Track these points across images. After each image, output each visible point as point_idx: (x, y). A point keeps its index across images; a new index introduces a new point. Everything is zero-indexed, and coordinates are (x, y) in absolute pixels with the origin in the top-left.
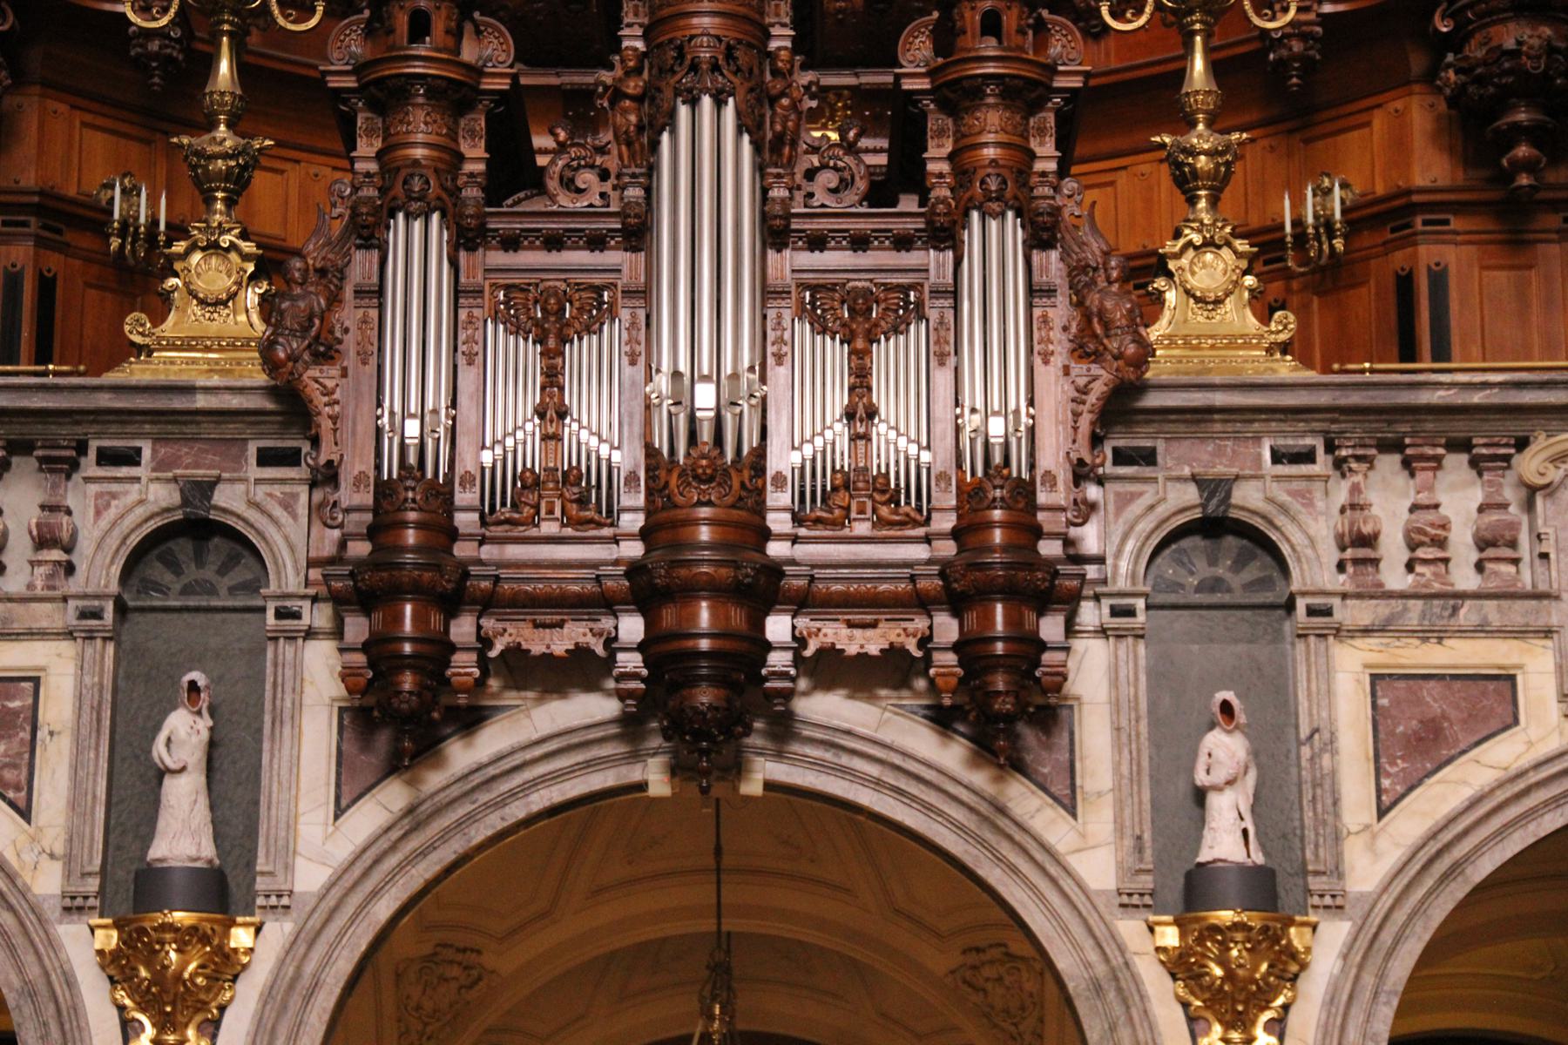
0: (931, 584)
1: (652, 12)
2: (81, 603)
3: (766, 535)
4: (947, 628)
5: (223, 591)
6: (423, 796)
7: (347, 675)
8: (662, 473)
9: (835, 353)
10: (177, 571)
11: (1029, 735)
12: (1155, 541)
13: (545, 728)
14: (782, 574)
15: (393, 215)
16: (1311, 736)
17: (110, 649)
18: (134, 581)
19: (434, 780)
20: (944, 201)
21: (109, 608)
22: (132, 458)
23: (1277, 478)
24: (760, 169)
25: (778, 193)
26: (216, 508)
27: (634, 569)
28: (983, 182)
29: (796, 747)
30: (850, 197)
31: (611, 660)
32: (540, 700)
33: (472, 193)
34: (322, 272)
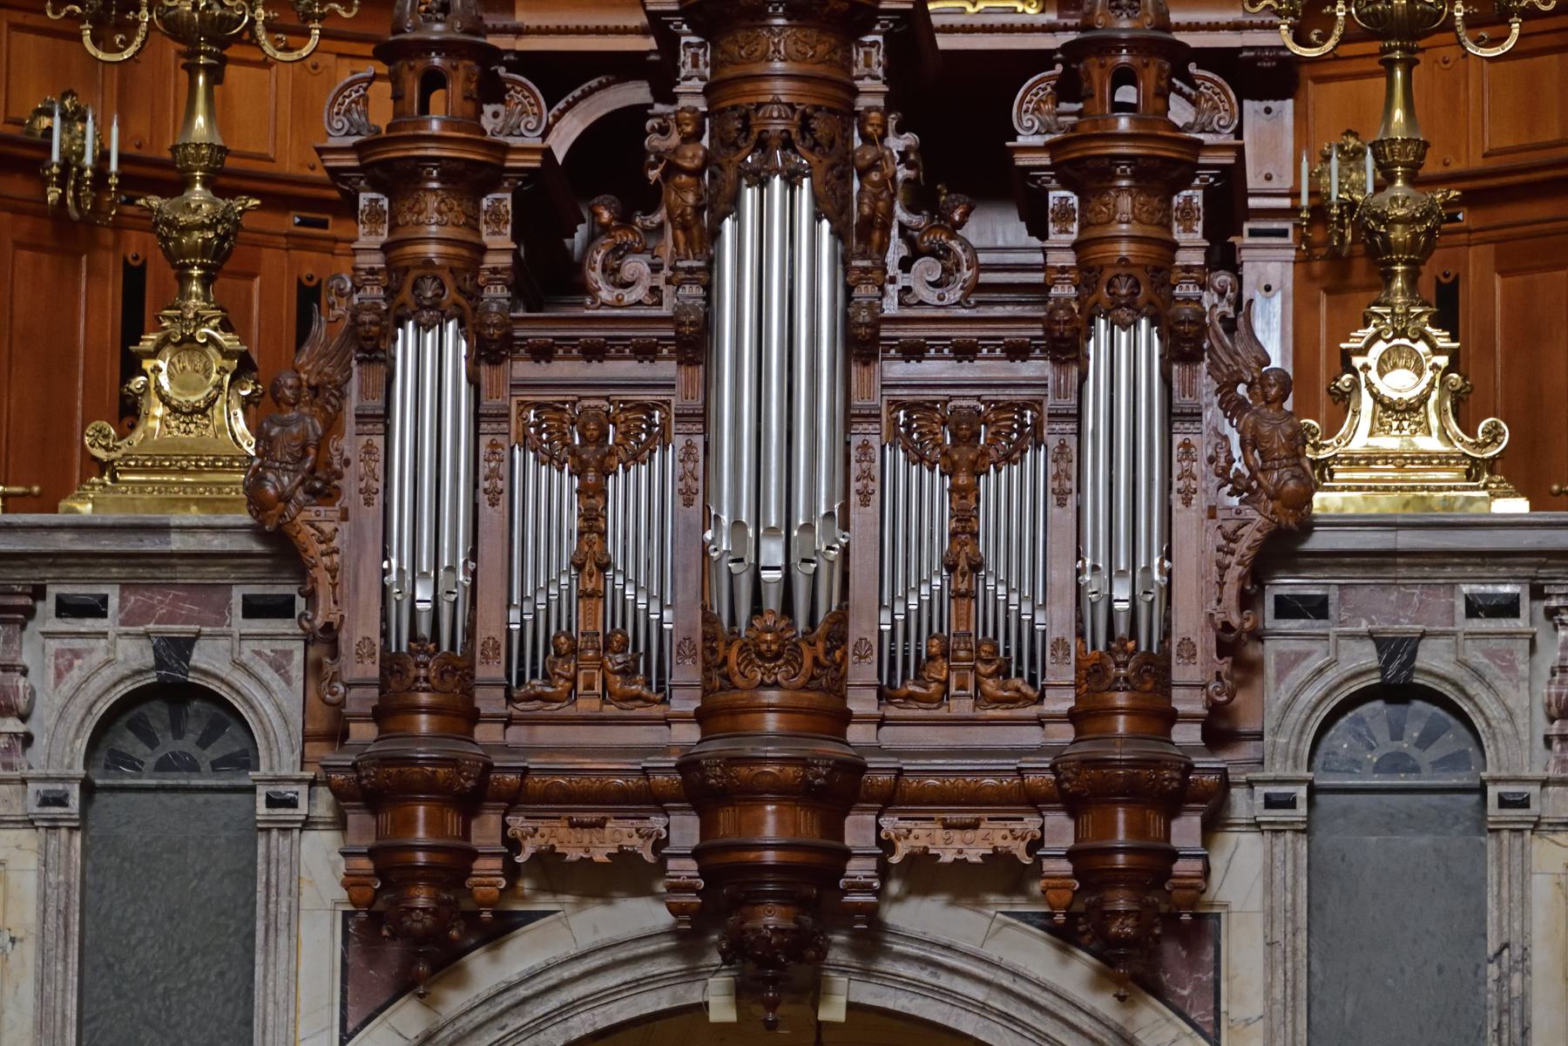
0: (1040, 779)
1: (715, 65)
2: (43, 787)
3: (847, 718)
4: (1060, 830)
5: (206, 767)
6: (442, 1021)
7: (351, 881)
8: (721, 647)
9: (937, 483)
10: (152, 742)
11: (1172, 951)
12: (1323, 712)
13: (587, 941)
14: (863, 768)
15: (401, 323)
16: (1499, 954)
17: (77, 839)
18: (102, 755)
19: (455, 1001)
20: (1063, 303)
21: (75, 792)
22: (96, 609)
23: (1471, 635)
24: (843, 261)
25: (864, 292)
26: (196, 669)
27: (689, 765)
28: (1110, 285)
29: (886, 965)
30: (954, 294)
31: (660, 868)
32: (579, 906)
33: (497, 293)
34: (315, 390)
